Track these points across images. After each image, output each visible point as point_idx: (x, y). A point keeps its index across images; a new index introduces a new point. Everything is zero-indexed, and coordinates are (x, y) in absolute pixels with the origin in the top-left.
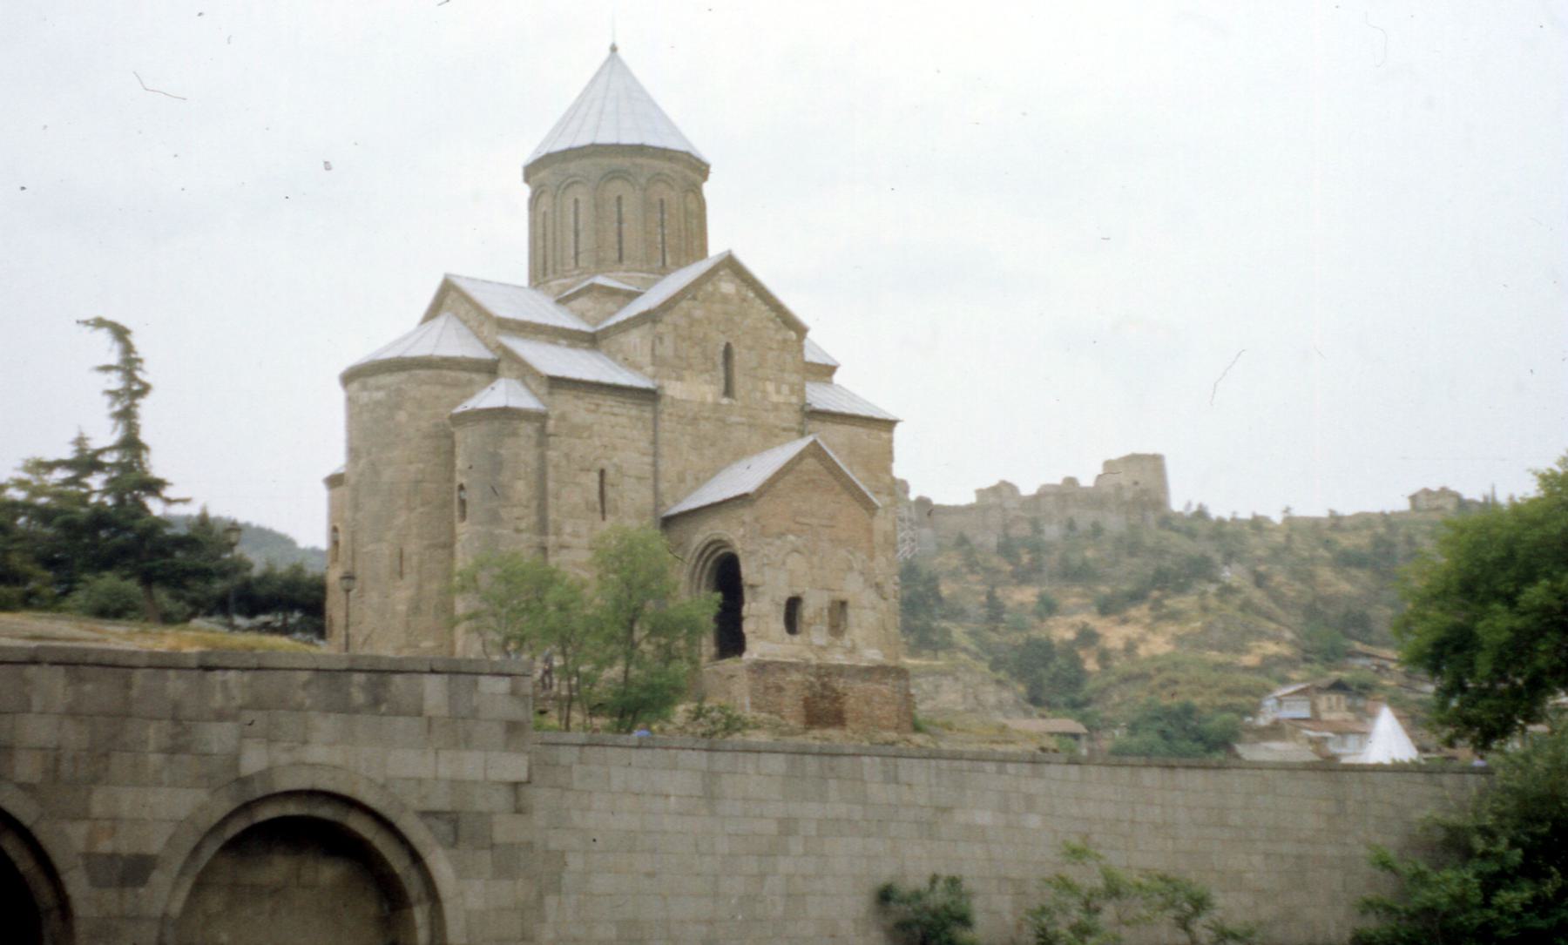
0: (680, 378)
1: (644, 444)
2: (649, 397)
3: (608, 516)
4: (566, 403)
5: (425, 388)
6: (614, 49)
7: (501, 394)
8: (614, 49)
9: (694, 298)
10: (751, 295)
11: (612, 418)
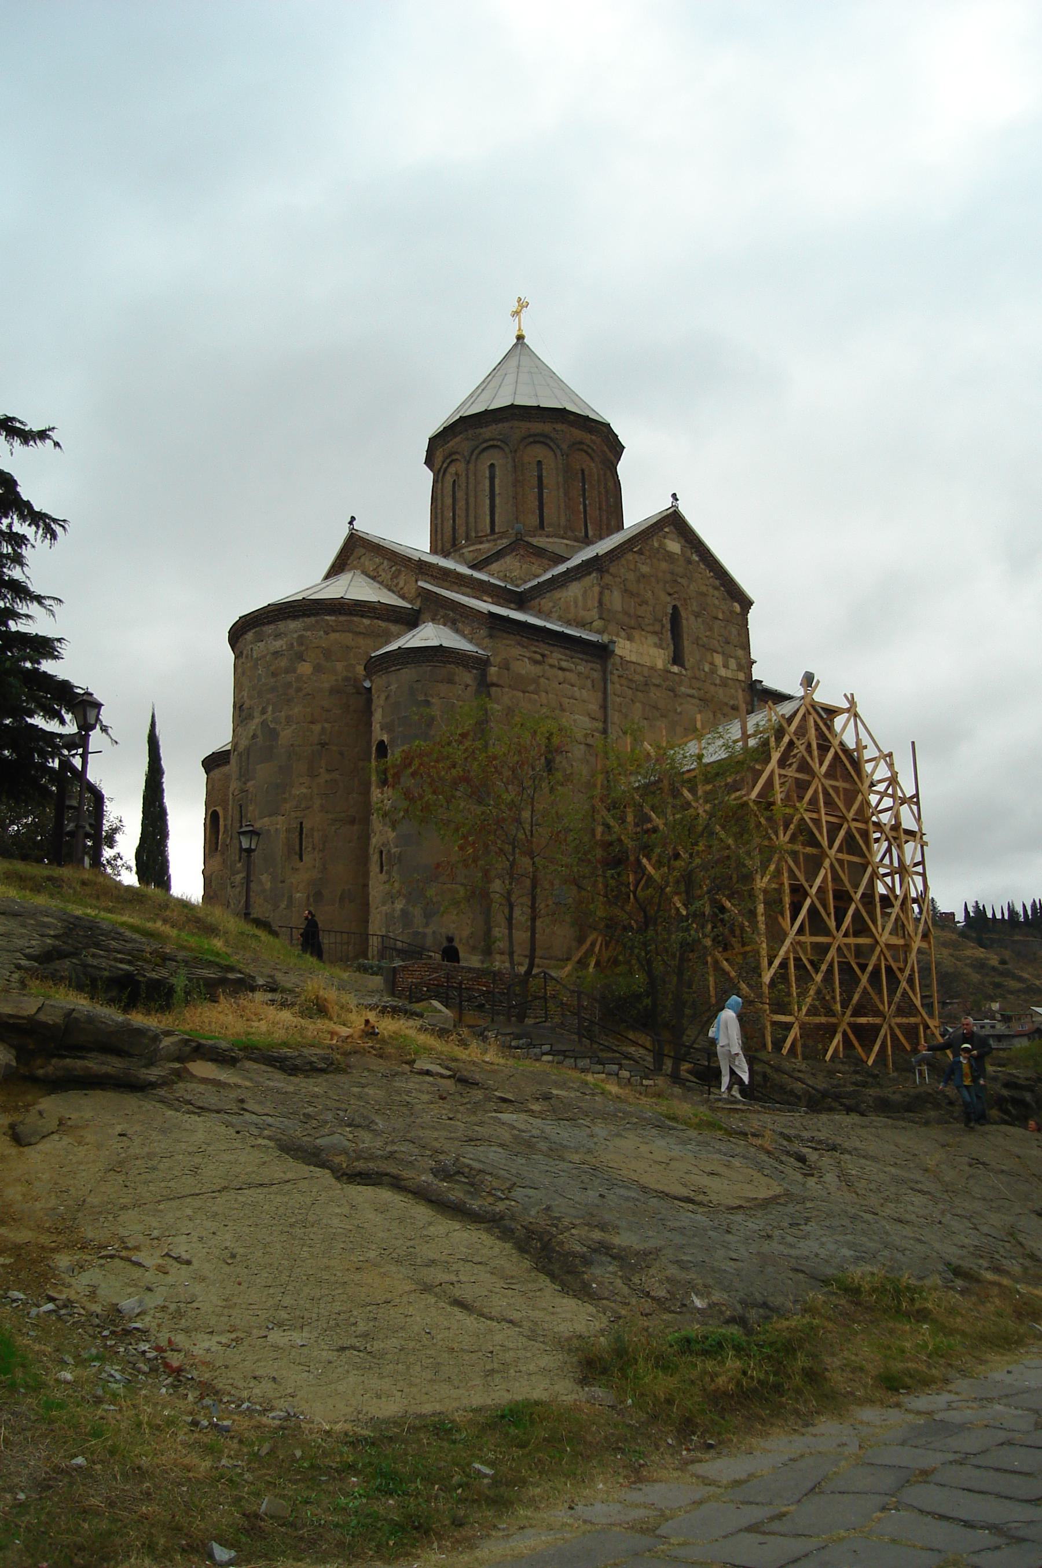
0: (630, 638)
1: (594, 707)
2: (601, 652)
4: (510, 650)
5: (333, 636)
6: (520, 338)
7: (429, 635)
8: (520, 338)
9: (640, 552)
10: (696, 558)
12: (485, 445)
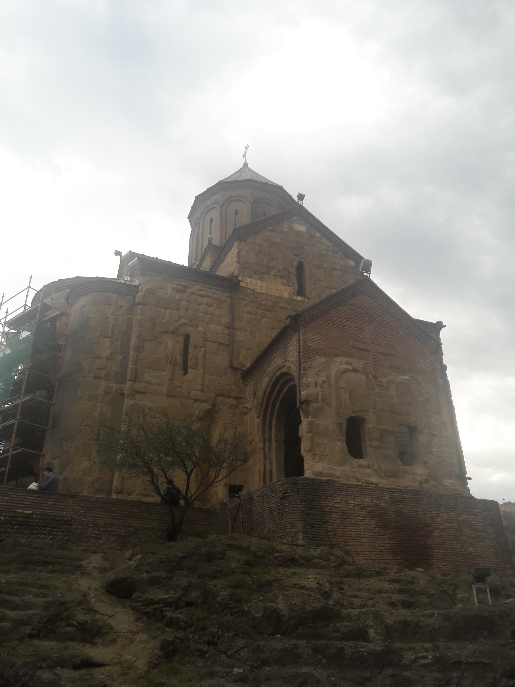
0: (262, 279)
3: (190, 371)
10: (318, 235)
11: (199, 298)
12: (208, 209)
